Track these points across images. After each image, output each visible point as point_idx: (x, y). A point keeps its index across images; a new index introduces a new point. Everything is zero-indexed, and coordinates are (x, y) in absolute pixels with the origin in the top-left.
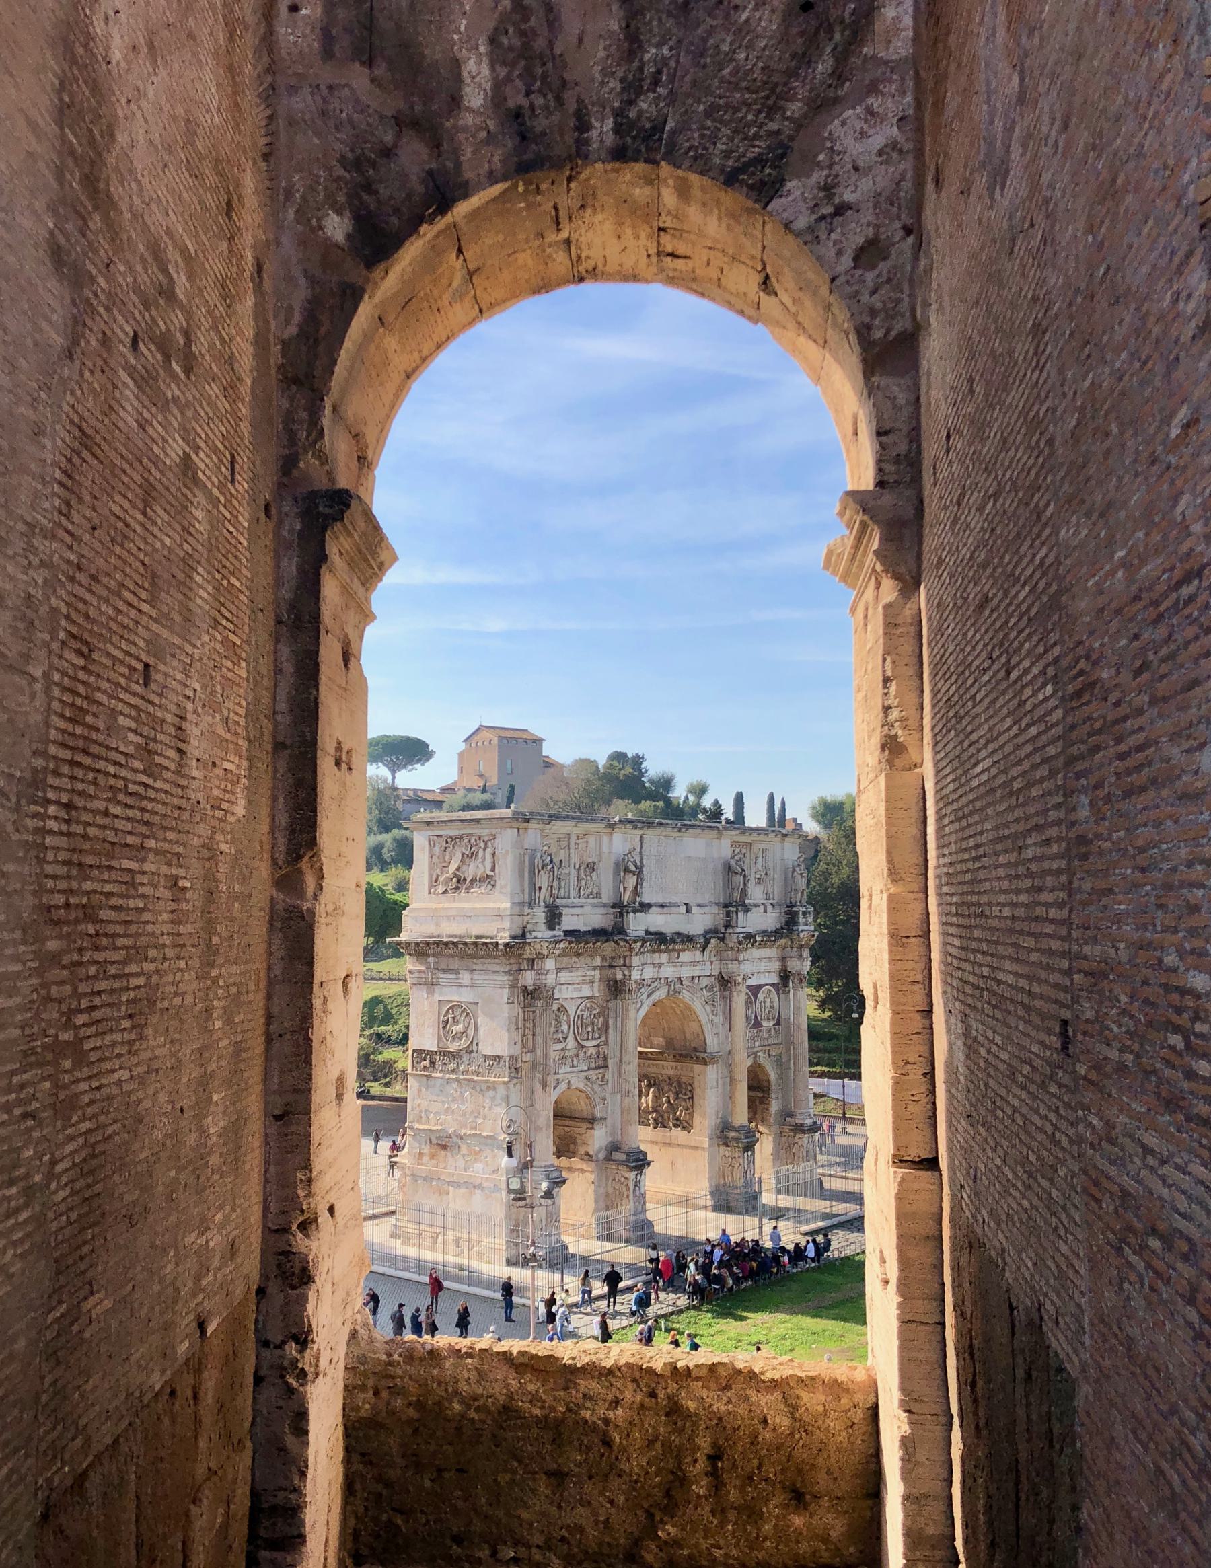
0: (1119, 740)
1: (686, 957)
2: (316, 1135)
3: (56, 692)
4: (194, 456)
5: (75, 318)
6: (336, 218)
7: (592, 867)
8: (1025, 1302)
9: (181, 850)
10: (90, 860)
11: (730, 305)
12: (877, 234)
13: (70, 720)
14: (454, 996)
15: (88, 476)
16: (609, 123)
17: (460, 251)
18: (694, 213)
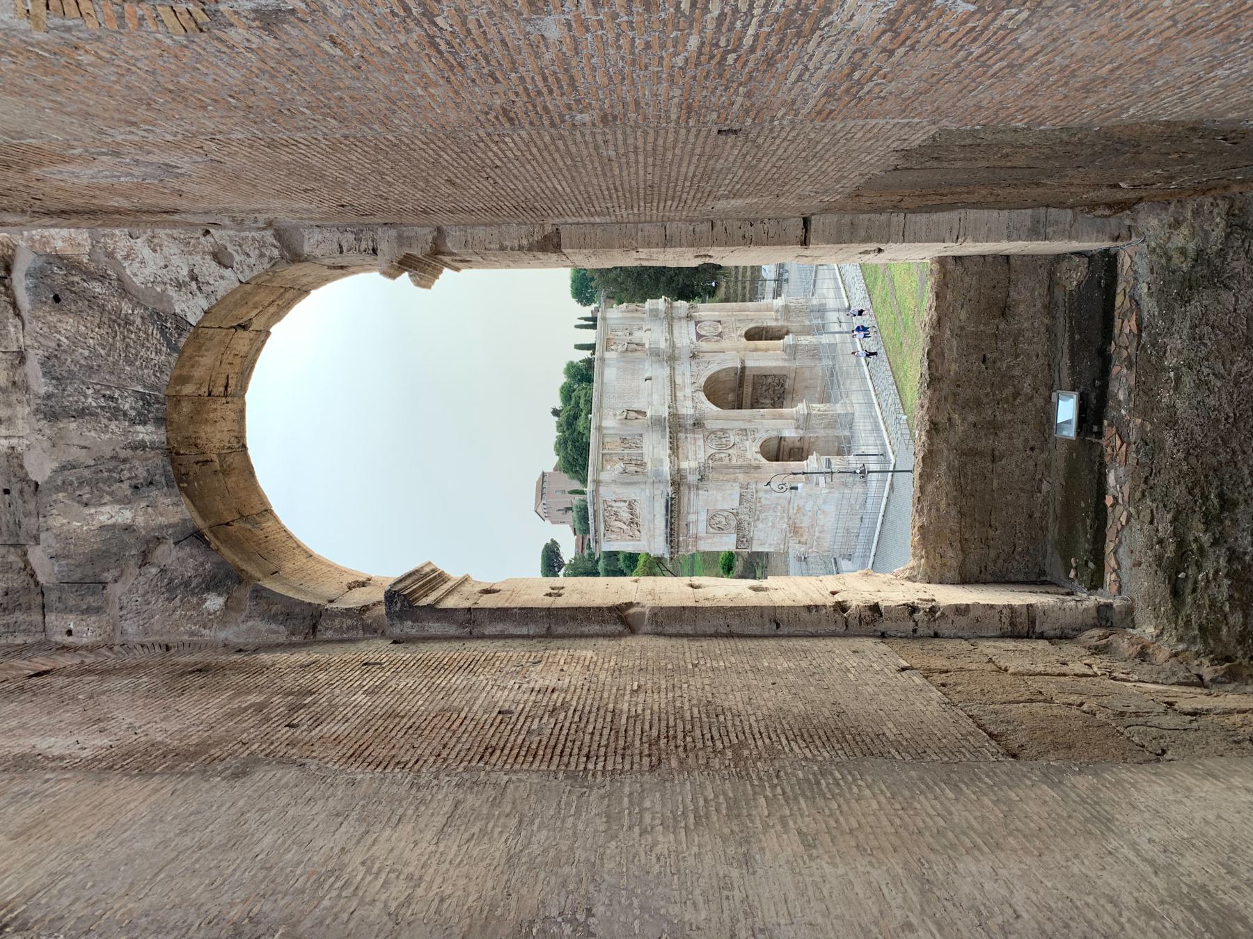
0: (539, 93)
1: (678, 380)
2: (788, 603)
3: (517, 766)
4: (366, 688)
5: (278, 763)
6: (208, 603)
7: (623, 440)
8: (893, 161)
9: (615, 689)
10: (621, 743)
11: (259, 350)
12: (210, 253)
13: (534, 758)
14: (702, 527)
15: (380, 752)
16: (139, 428)
17: (227, 524)
18: (198, 373)
